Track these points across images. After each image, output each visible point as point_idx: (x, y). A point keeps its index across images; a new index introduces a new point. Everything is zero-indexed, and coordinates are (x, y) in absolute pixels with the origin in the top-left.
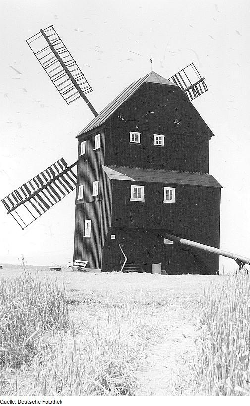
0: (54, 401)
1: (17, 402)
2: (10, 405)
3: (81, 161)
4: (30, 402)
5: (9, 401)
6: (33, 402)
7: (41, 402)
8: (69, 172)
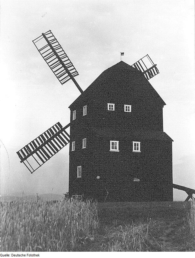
1: (11, 255)
3: (72, 124)
4: (19, 256)
5: (5, 255)
6: (21, 256)
8: (63, 132)
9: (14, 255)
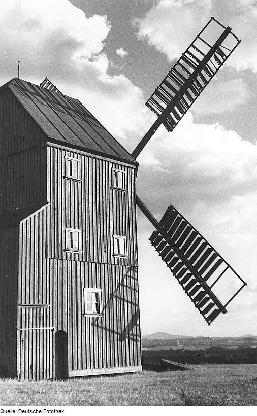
0: (55, 411)
1: (17, 412)
2: (10, 414)
4: (31, 412)
5: (9, 411)
6: (34, 412)
7: (42, 412)
9: (23, 412)
